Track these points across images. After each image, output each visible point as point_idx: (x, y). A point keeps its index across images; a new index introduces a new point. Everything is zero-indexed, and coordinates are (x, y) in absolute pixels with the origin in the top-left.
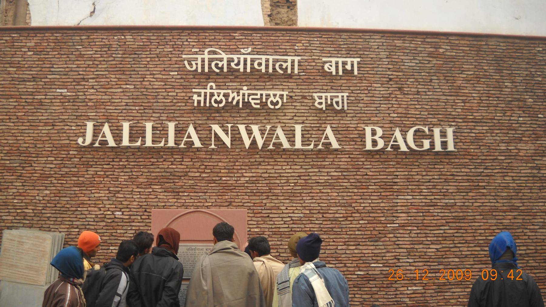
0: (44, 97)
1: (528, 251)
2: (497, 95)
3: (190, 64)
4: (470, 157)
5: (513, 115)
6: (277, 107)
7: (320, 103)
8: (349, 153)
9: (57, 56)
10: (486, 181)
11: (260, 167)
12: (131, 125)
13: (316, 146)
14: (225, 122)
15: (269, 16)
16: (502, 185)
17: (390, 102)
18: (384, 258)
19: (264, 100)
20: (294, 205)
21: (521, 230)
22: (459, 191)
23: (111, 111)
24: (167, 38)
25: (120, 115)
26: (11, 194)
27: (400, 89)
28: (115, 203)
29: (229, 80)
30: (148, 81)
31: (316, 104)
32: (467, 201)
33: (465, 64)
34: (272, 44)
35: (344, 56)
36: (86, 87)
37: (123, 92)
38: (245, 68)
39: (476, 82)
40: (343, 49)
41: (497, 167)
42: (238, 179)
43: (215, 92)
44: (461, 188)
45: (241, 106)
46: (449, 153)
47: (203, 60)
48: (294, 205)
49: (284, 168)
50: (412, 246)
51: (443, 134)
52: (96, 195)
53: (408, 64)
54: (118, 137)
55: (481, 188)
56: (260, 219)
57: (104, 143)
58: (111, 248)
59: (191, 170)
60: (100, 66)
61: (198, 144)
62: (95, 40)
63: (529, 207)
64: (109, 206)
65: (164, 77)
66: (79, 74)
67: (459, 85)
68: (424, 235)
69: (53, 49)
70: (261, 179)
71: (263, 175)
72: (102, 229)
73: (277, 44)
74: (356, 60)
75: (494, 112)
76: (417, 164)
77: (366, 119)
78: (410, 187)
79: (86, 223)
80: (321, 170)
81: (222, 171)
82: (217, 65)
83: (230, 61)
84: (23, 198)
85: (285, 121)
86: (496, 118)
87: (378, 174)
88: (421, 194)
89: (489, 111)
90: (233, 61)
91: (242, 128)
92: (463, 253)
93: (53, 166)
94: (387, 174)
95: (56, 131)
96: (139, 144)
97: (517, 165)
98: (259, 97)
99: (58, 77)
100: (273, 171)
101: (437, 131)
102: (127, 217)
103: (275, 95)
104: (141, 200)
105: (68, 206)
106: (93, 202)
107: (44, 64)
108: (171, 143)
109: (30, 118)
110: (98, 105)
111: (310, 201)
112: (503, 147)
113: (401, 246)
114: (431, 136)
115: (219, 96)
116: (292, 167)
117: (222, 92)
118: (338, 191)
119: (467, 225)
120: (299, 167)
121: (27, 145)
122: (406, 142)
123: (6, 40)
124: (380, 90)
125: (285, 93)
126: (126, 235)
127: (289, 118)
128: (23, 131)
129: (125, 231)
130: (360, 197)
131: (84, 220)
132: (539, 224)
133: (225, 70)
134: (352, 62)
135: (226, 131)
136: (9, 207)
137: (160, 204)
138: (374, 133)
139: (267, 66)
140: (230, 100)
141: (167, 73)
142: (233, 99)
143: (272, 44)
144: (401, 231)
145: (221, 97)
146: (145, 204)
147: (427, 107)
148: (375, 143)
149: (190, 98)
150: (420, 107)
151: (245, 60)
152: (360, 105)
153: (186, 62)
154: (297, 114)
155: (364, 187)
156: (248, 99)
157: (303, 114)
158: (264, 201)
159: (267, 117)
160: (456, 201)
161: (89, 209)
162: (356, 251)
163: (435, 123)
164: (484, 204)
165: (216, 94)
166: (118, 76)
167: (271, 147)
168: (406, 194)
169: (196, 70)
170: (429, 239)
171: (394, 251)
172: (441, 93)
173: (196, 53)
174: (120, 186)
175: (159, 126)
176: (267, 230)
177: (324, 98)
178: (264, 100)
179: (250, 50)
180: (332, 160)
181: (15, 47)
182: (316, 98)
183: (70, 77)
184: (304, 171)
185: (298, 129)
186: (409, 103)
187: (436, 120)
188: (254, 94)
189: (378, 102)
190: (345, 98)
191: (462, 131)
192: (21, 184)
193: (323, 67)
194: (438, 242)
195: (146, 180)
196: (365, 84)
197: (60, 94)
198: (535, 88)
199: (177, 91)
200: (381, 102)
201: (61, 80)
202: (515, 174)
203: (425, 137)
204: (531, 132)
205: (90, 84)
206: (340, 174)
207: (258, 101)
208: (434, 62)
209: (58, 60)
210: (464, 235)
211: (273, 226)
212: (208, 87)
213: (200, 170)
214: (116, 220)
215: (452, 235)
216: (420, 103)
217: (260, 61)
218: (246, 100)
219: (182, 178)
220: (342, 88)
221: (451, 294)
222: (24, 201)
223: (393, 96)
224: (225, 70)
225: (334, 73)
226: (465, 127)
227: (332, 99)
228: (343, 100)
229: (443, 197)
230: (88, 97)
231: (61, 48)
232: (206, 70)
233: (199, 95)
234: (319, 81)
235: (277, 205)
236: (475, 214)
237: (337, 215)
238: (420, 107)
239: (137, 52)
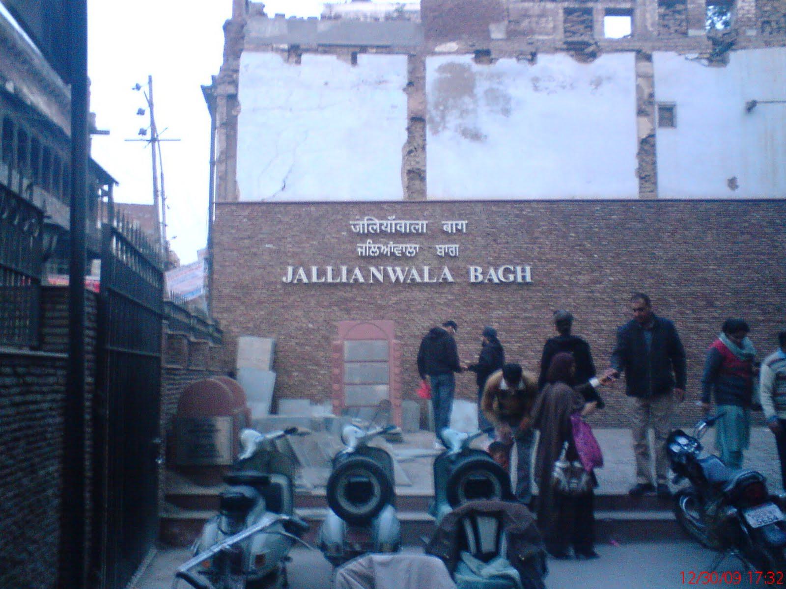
6: (413, 255)
7: (441, 252)
8: (460, 284)
15: (407, 187)
19: (404, 250)
22: (534, 307)
27: (495, 240)
43: (372, 246)
46: (528, 284)
47: (363, 225)
51: (523, 271)
54: (309, 275)
57: (300, 280)
61: (361, 280)
69: (261, 217)
74: (465, 222)
82: (372, 228)
83: (381, 225)
91: (390, 269)
101: (519, 269)
103: (411, 248)
108: (344, 280)
110: (295, 255)
112: (567, 278)
114: (514, 272)
117: (377, 246)
122: (497, 276)
124: (481, 241)
125: (418, 246)
133: (378, 231)
134: (462, 225)
135: (379, 271)
138: (476, 270)
139: (405, 228)
140: (382, 251)
142: (384, 250)
145: (376, 249)
148: (476, 277)
149: (355, 250)
151: (391, 225)
153: (352, 227)
156: (394, 250)
167: (409, 281)
173: (358, 220)
188: (397, 247)
190: (457, 249)
193: (443, 227)
196: (471, 237)
218: (392, 250)
225: (450, 231)
227: (448, 250)
228: (456, 249)
233: (362, 248)
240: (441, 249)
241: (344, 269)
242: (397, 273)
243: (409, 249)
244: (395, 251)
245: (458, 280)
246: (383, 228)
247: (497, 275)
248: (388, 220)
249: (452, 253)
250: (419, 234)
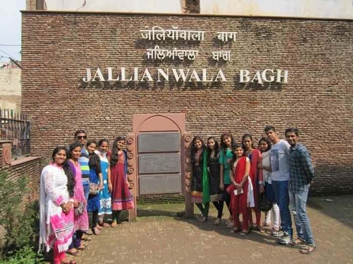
0: (60, 53)
1: (325, 135)
6: (193, 59)
7: (216, 57)
13: (214, 80)
30: (121, 44)
34: (189, 24)
43: (159, 50)
45: (173, 58)
47: (152, 33)
66: (80, 40)
72: (99, 126)
82: (159, 36)
83: (167, 33)
91: (174, 71)
98: (183, 53)
99: (68, 41)
100: (191, 94)
103: (192, 53)
117: (163, 51)
123: (33, 19)
125: (197, 51)
133: (164, 39)
139: (187, 36)
142: (169, 54)
143: (189, 24)
145: (163, 53)
151: (175, 33)
152: (237, 58)
153: (142, 34)
165: (159, 52)
166: (103, 41)
169: (148, 39)
173: (147, 29)
179: (177, 27)
187: (277, 66)
188: (180, 52)
203: (272, 75)
223: (254, 53)
224: (164, 39)
225: (223, 40)
227: (222, 55)
230: (87, 53)
232: (154, 39)
237: (225, 117)
241: (136, 70)
242: (180, 74)
243: (190, 54)
244: (179, 55)
246: (168, 35)
248: (174, 29)
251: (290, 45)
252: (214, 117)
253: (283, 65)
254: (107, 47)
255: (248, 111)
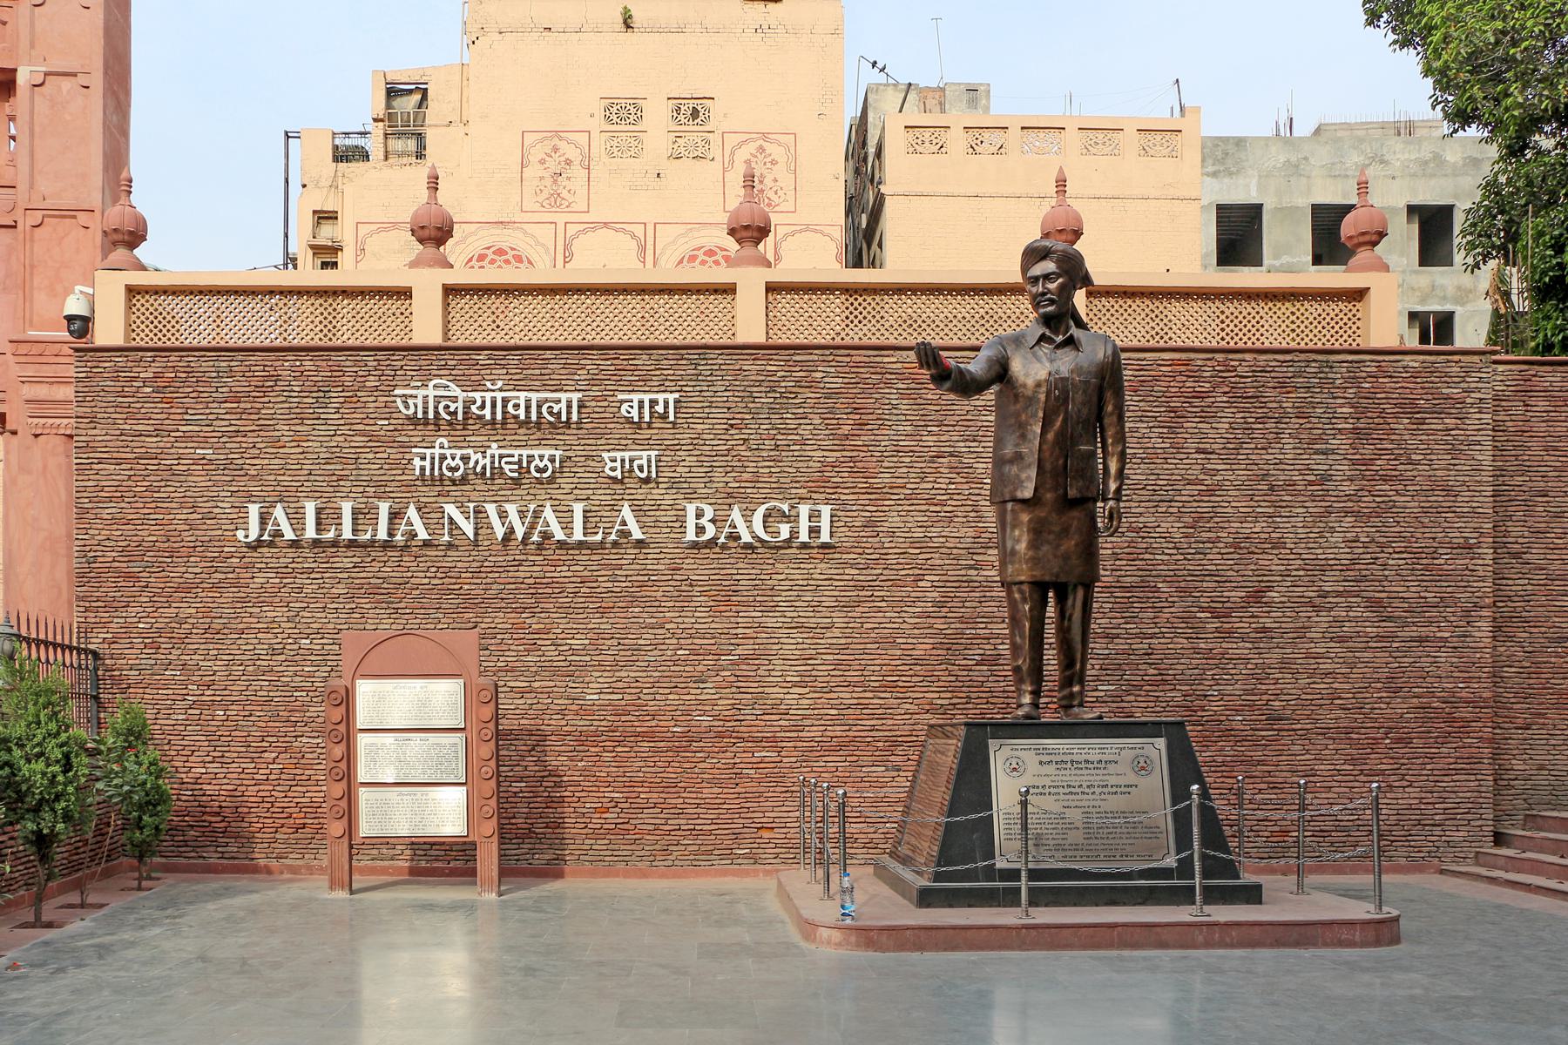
2: (912, 448)
3: (407, 407)
4: (861, 550)
5: (938, 480)
6: (545, 475)
7: (613, 469)
9: (191, 395)
10: (886, 589)
11: (521, 568)
12: (319, 506)
14: (466, 499)
16: (913, 594)
17: (730, 464)
18: (715, 708)
19: (525, 465)
20: (575, 626)
21: (943, 667)
23: (286, 484)
24: (369, 364)
25: (300, 489)
26: (133, 614)
28: (298, 626)
29: (471, 433)
31: (607, 470)
32: (853, 620)
33: (859, 396)
34: (538, 372)
35: (656, 389)
36: (244, 445)
37: (303, 453)
38: (494, 413)
39: (877, 427)
40: (654, 378)
41: (906, 567)
42: (488, 586)
43: (448, 452)
44: (843, 599)
48: (575, 626)
49: (559, 569)
50: (760, 690)
51: (814, 515)
52: (269, 614)
53: (762, 400)
55: (877, 599)
56: (521, 648)
58: (295, 694)
59: (415, 574)
60: (263, 411)
62: (253, 368)
63: (959, 631)
64: (290, 631)
65: (367, 428)
67: (847, 433)
68: (780, 673)
70: (523, 586)
71: (526, 581)
73: (547, 371)
74: (671, 397)
75: (905, 475)
76: (771, 561)
77: (688, 491)
78: (758, 598)
79: (256, 657)
80: (616, 572)
81: (463, 575)
84: (154, 620)
85: (559, 497)
86: (908, 486)
87: (707, 578)
88: (777, 609)
89: (896, 475)
90: (475, 402)
91: (491, 509)
92: (845, 701)
93: (199, 570)
94: (721, 577)
95: (200, 516)
96: (331, 535)
97: (942, 562)
99: (197, 428)
101: (804, 510)
102: (319, 647)
103: (541, 457)
104: (339, 621)
105: (226, 631)
106: (265, 626)
107: (172, 407)
109: (155, 495)
111: (599, 621)
113: (742, 690)
114: (792, 519)
115: (453, 459)
116: (571, 568)
117: (459, 453)
118: (642, 604)
119: (852, 657)
120: (582, 568)
121: (154, 538)
125: (558, 453)
126: (317, 674)
127: (565, 491)
128: (147, 516)
129: (316, 669)
130: (678, 614)
131: (252, 653)
132: (976, 657)
133: (460, 417)
134: (666, 403)
136: (132, 635)
137: (368, 627)
138: (700, 515)
139: (528, 408)
140: (471, 465)
141: (372, 422)
142: (477, 462)
143: (538, 372)
144: (744, 667)
145: (458, 461)
146: (346, 626)
147: (790, 470)
150: (778, 470)
152: (678, 469)
154: (578, 486)
155: (686, 599)
156: (500, 463)
157: (587, 486)
158: (528, 621)
159: (531, 491)
160: (835, 620)
161: (259, 636)
162: (671, 697)
163: (803, 496)
164: (882, 626)
168: (752, 609)
170: (788, 679)
171: (731, 696)
172: (815, 447)
174: (307, 600)
175: (363, 506)
176: (532, 664)
177: (619, 461)
178: (525, 465)
180: (633, 557)
181: (121, 379)
182: (607, 461)
183: (217, 429)
184: (590, 574)
185: (578, 508)
186: (760, 464)
187: (806, 491)
188: (509, 456)
189: (709, 464)
191: (849, 508)
192: (147, 599)
194: (803, 684)
195: (346, 591)
197: (202, 456)
198: (981, 433)
199: (389, 450)
200: (714, 464)
201: (202, 434)
202: (937, 578)
204: (970, 508)
205: (250, 440)
206: (646, 578)
207: (516, 467)
208: (806, 396)
209: (194, 400)
210: (846, 673)
211: (543, 659)
212: (437, 445)
213: (428, 575)
214: (301, 651)
215: (826, 673)
216: (780, 464)
217: (517, 401)
218: (497, 465)
219: (402, 587)
220: (651, 442)
221: (823, 764)
222: (155, 625)
224: (460, 417)
226: (854, 502)
229: (812, 614)
230: (248, 461)
231: (197, 381)
233: (423, 459)
234: (615, 431)
235: (548, 626)
236: (866, 640)
238: (778, 470)
239: (322, 389)
240: (612, 461)
245: (660, 538)
247: (749, 526)
249: (641, 470)
250: (560, 425)
251: (846, 429)
252: (609, 642)
253: (820, 486)
254: (305, 444)
255: (713, 625)
